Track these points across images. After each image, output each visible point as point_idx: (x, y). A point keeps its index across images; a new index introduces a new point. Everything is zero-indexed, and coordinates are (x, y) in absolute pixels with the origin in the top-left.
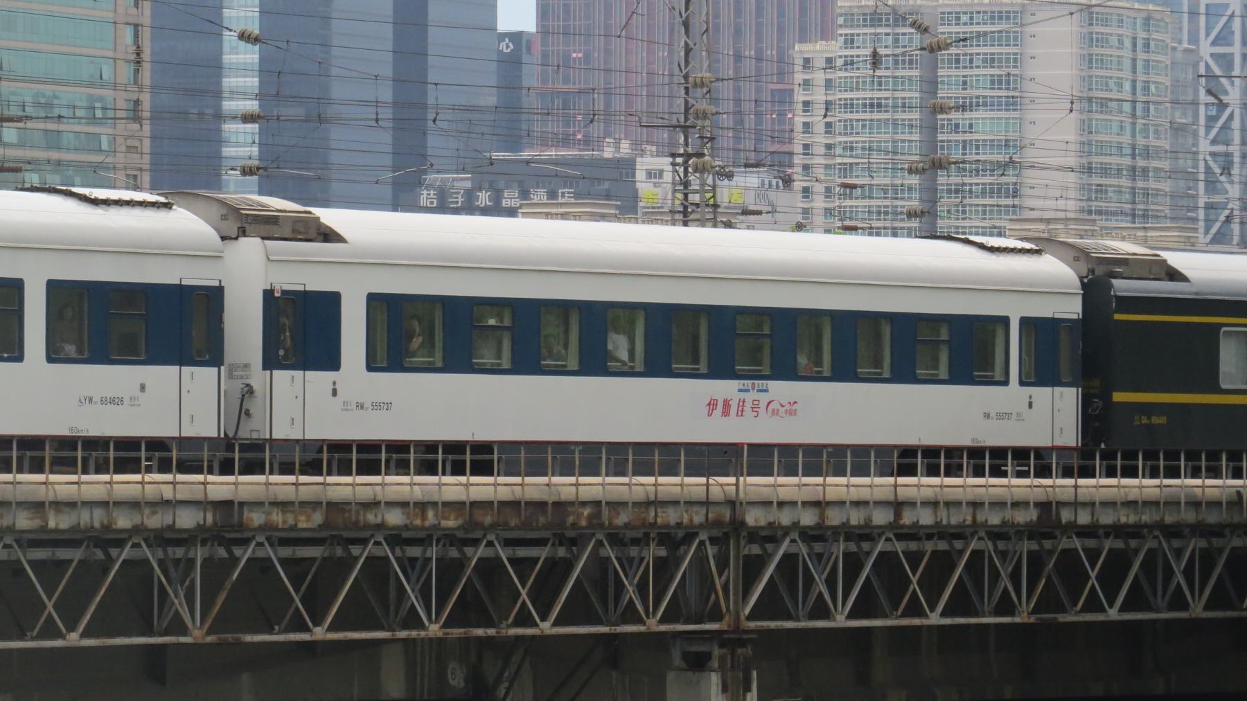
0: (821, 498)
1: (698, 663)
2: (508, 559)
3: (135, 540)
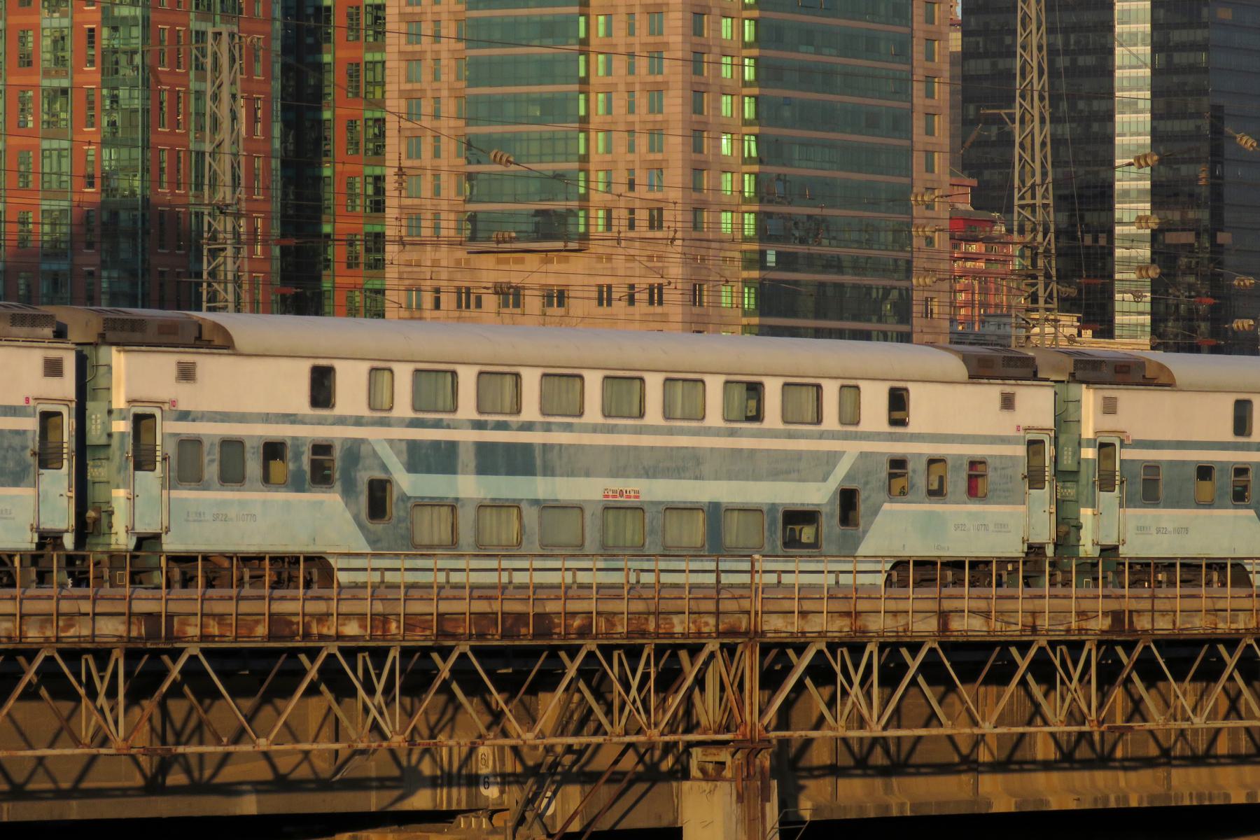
1: (714, 774)
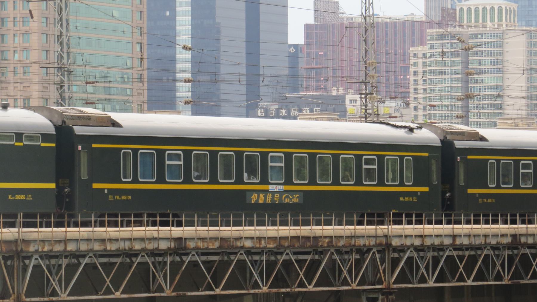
0: (423, 234)
2: (295, 260)
3: (143, 254)
